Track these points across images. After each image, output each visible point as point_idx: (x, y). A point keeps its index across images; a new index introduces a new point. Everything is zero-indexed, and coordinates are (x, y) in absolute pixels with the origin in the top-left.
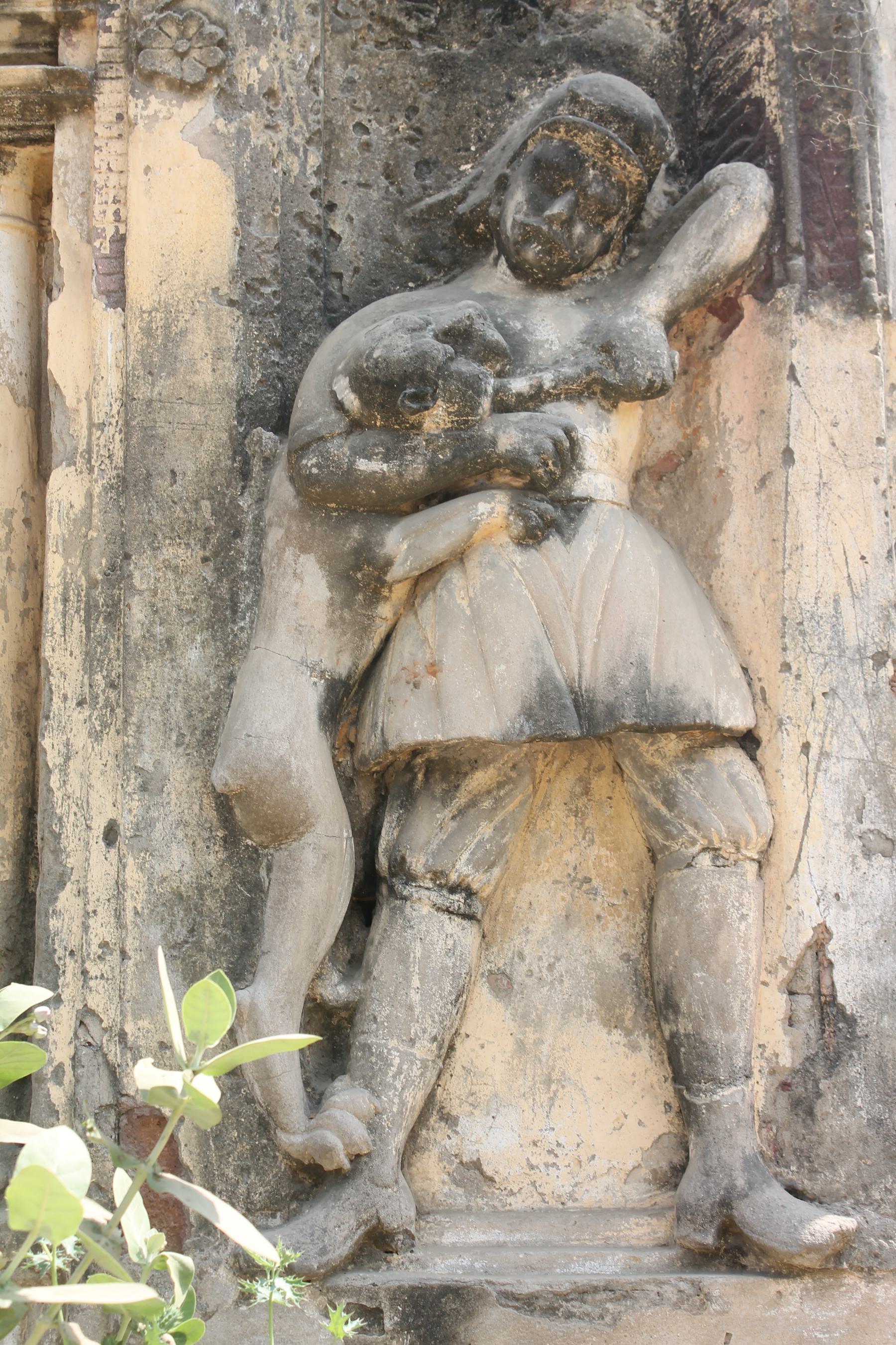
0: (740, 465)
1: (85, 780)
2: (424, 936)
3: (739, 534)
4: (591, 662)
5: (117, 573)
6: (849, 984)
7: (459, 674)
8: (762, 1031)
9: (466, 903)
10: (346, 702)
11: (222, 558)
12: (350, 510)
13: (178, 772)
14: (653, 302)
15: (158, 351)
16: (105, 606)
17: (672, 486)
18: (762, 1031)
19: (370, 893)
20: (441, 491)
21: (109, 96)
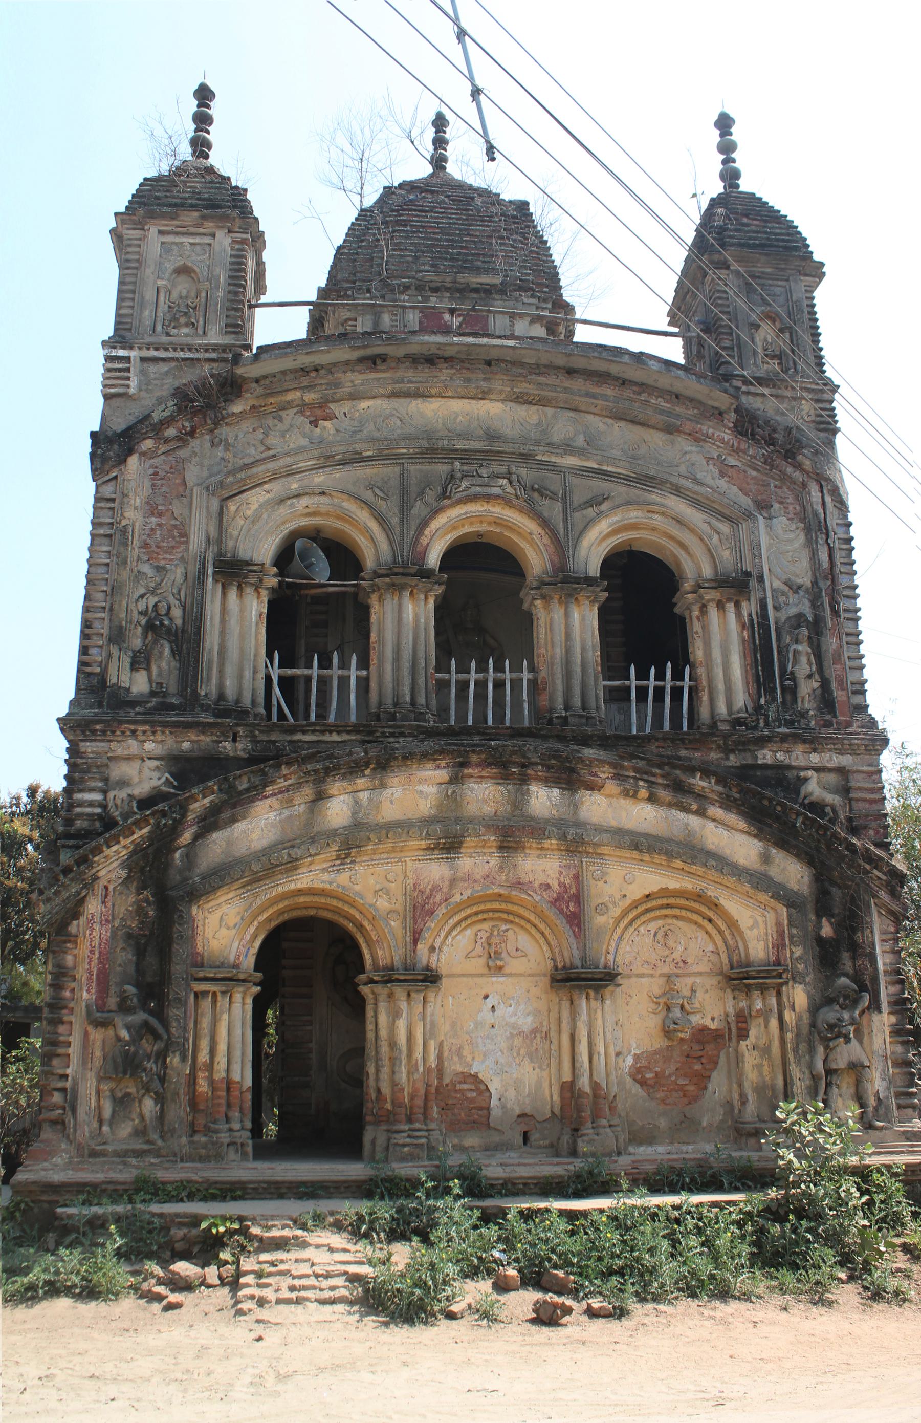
0: (866, 1032)
1: (796, 1072)
2: (835, 1090)
3: (866, 1039)
4: (854, 1059)
5: (797, 1046)
6: (881, 1096)
7: (839, 1060)
8: (872, 1101)
9: (838, 1087)
10: (825, 1061)
11: (809, 1045)
12: (826, 1041)
13: (807, 1072)
14: (857, 1012)
15: (799, 1018)
16: (796, 1050)
17: (858, 1032)
18: (872, 1101)
19: (828, 1085)
20: (837, 1037)
21: (791, 983)
